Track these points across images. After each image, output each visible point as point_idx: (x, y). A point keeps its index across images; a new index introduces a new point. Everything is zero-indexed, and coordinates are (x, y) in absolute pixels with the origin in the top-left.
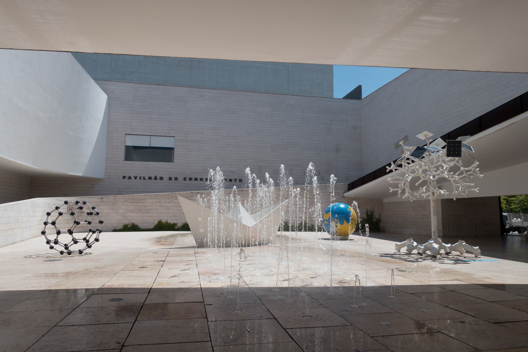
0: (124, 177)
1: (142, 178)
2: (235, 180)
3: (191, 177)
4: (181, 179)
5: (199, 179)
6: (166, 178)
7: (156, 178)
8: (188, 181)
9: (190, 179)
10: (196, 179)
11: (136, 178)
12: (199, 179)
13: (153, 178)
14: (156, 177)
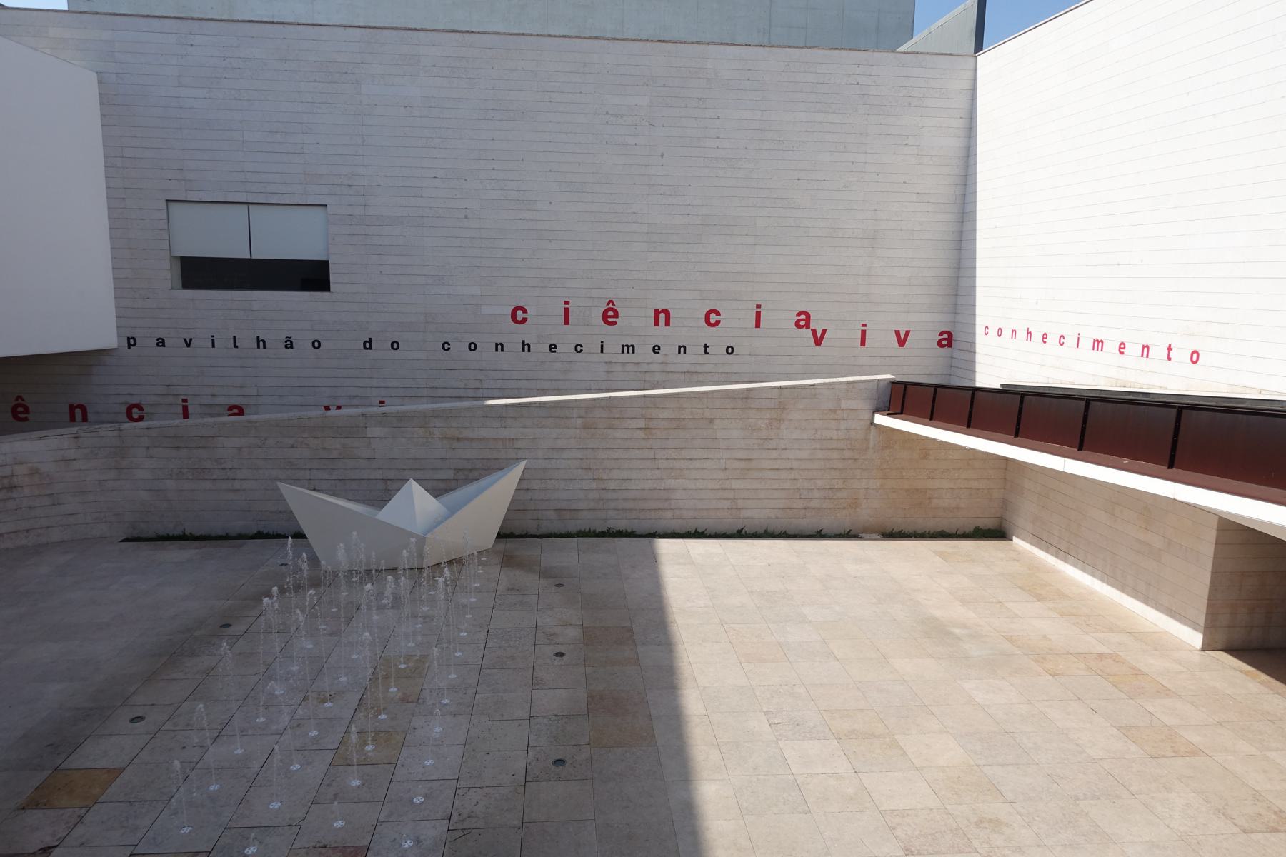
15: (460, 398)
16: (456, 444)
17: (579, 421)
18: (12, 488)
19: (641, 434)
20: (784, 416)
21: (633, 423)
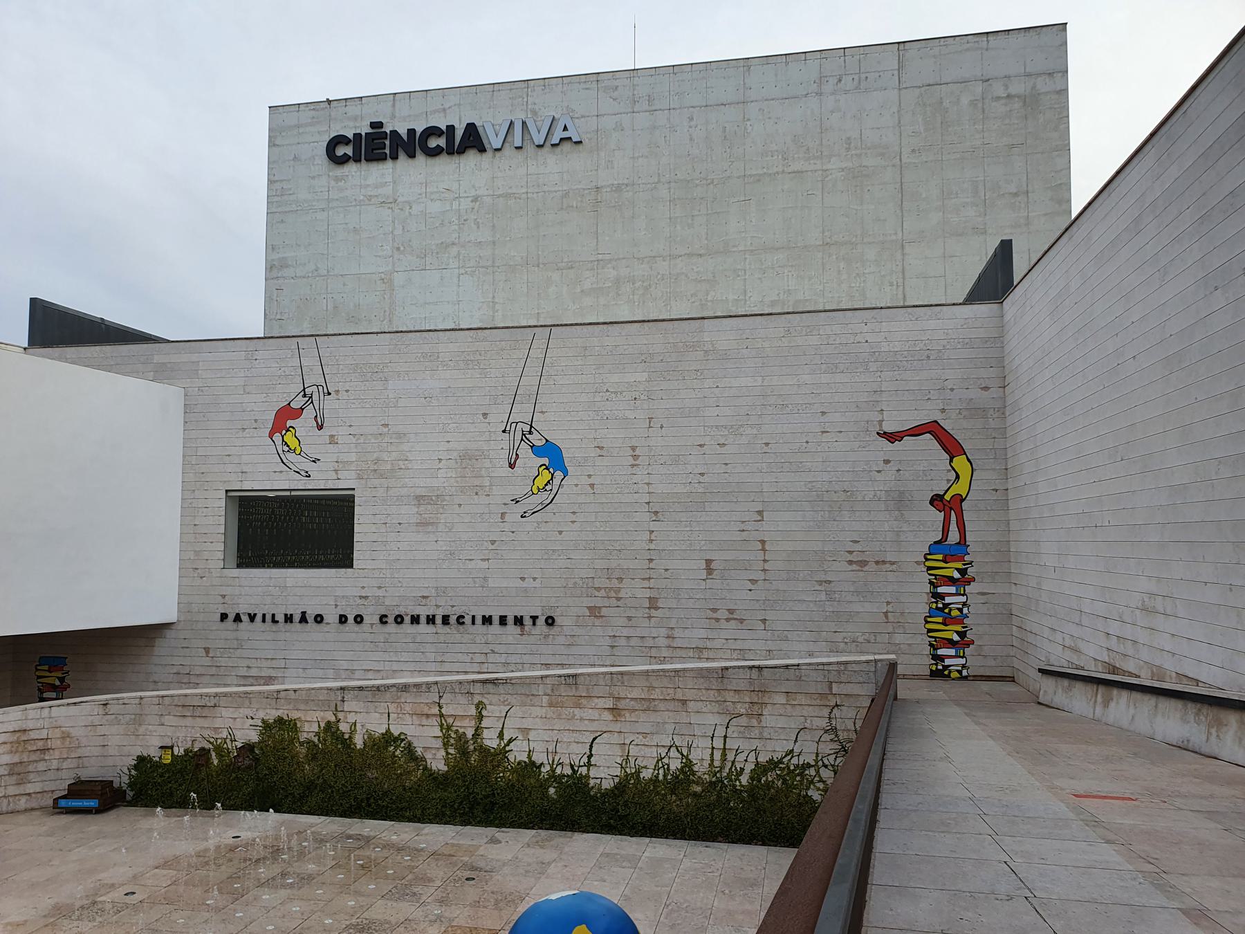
0: (224, 617)
1: (268, 618)
2: (534, 618)
3: (401, 611)
4: (371, 618)
5: (423, 619)
6: (331, 617)
7: (303, 619)
8: (392, 627)
9: (399, 620)
10: (415, 620)
11: (252, 618)
12: (423, 619)
13: (297, 618)
14: (304, 613)
15: (466, 673)
16: (425, 722)
17: (545, 699)
18: (44, 750)
19: (607, 716)
20: (766, 700)
21: (601, 703)
